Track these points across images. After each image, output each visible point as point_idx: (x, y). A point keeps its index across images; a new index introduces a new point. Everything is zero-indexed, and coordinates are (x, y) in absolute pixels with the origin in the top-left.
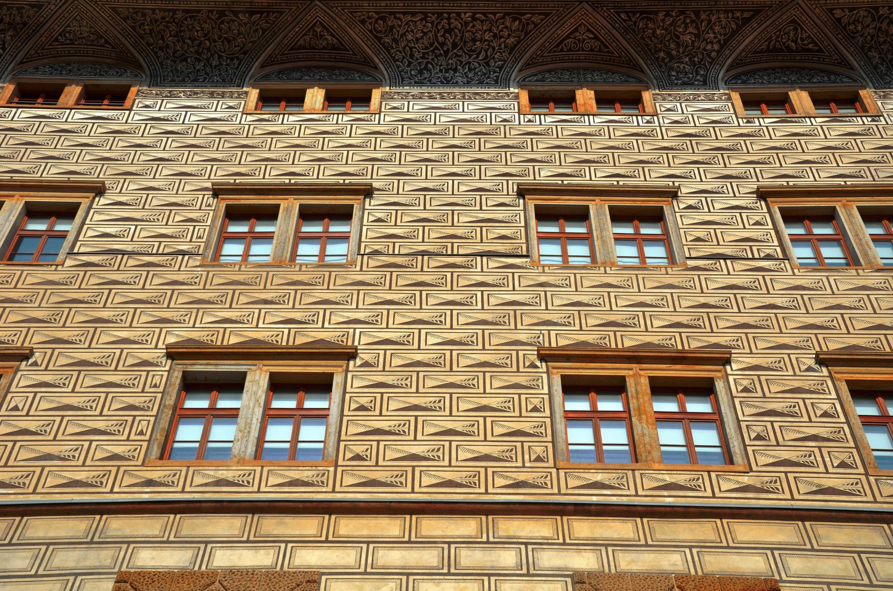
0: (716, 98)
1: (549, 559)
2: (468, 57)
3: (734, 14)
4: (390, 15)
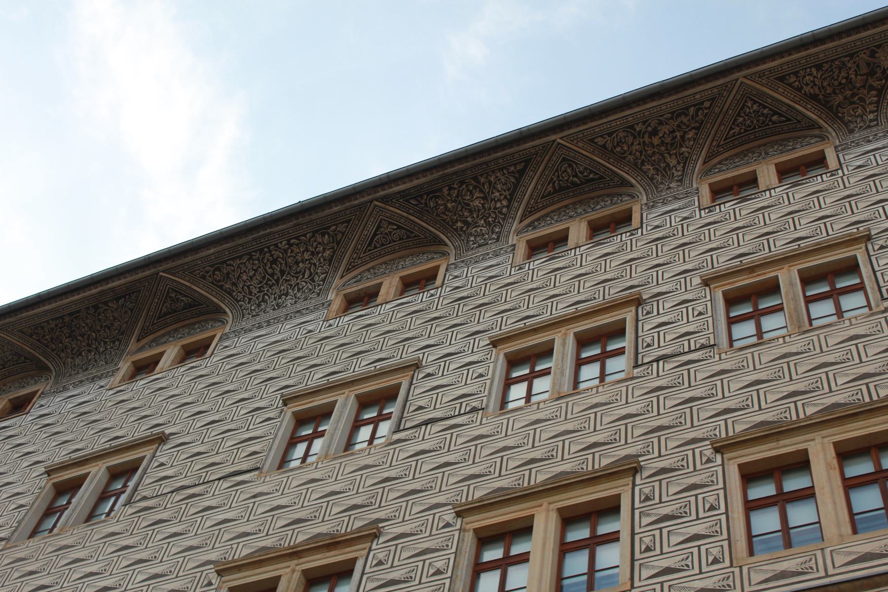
0: (502, 252)
2: (295, 279)
3: (508, 170)
4: (223, 264)
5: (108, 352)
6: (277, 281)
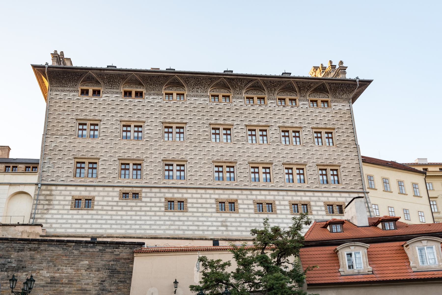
1: (213, 196)
5: (158, 87)
6: (197, 85)
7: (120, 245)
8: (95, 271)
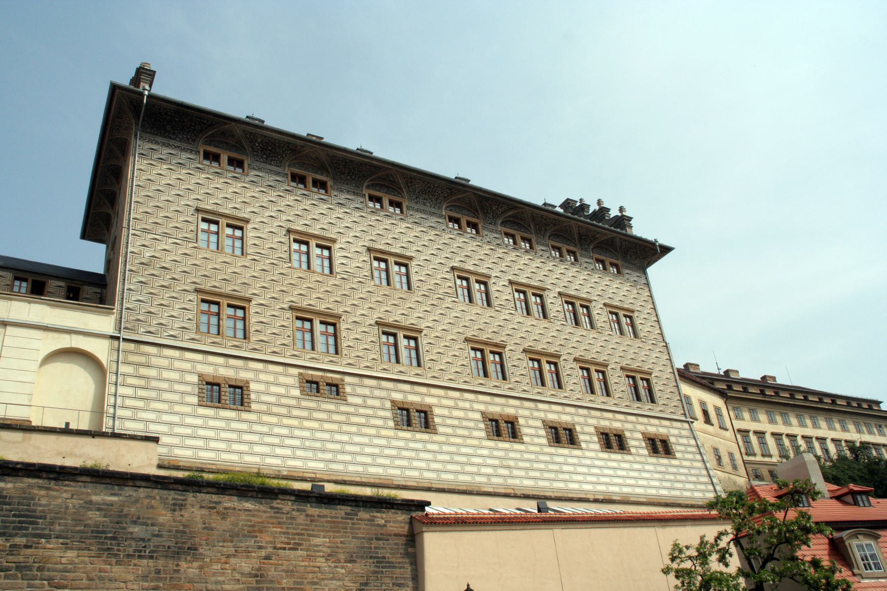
7: (384, 506)
8: (345, 562)
